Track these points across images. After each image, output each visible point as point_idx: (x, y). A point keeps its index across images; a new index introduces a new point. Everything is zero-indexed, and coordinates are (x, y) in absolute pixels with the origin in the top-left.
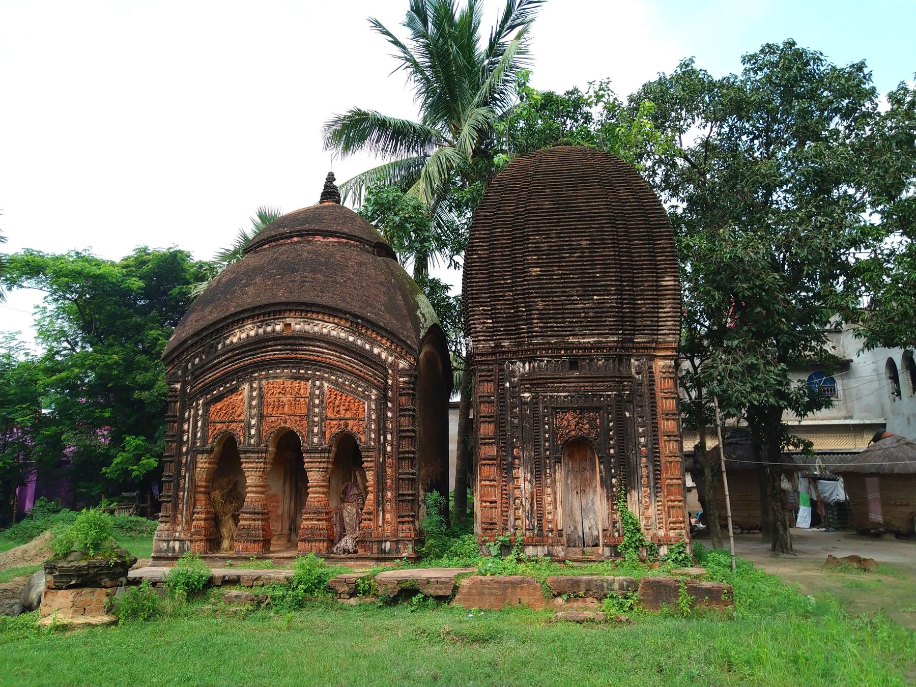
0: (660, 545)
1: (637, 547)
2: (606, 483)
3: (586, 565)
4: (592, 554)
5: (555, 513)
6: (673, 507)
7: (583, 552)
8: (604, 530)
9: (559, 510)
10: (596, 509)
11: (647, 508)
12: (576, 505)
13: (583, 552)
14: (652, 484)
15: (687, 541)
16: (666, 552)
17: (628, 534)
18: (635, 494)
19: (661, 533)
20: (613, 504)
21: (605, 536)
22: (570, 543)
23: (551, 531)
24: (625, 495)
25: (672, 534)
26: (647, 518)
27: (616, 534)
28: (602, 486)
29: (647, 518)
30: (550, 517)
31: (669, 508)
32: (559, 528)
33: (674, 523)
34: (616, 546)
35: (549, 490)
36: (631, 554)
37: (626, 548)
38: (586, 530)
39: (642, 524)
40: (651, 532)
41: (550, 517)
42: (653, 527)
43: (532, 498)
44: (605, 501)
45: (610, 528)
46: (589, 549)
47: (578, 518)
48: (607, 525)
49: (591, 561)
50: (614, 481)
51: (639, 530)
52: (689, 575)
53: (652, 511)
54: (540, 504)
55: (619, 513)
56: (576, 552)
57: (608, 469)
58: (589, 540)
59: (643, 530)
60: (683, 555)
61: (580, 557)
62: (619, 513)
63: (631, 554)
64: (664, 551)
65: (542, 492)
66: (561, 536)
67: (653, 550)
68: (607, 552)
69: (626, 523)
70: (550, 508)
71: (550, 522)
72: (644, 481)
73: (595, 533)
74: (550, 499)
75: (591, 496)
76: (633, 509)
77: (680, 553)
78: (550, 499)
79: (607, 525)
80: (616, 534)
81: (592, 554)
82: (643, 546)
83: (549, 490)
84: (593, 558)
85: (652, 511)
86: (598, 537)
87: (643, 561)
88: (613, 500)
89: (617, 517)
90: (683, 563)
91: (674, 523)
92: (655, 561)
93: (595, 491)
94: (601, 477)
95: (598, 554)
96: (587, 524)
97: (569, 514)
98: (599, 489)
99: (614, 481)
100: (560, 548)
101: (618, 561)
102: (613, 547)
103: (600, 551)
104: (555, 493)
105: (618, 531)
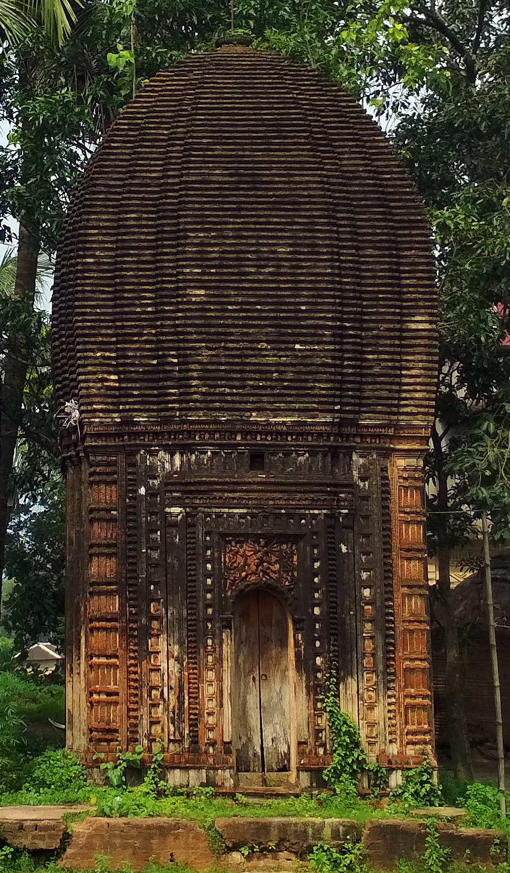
0: (390, 770)
1: (353, 774)
2: (304, 665)
3: (270, 801)
4: (280, 783)
5: (221, 713)
6: (413, 707)
7: (264, 782)
8: (300, 743)
9: (227, 709)
10: (286, 707)
11: (371, 708)
12: (252, 701)
13: (264, 782)
14: (381, 667)
15: (435, 763)
16: (400, 782)
17: (340, 751)
18: (352, 683)
19: (393, 750)
20: (317, 701)
21: (301, 754)
22: (242, 765)
23: (213, 744)
24: (337, 685)
25: (410, 751)
26: (371, 725)
27: (321, 751)
28: (298, 668)
29: (371, 725)
30: (211, 720)
31: (406, 708)
32: (226, 739)
33: (414, 733)
34: (319, 771)
35: (211, 675)
36: (346, 785)
37: (337, 774)
38: (268, 743)
39: (363, 733)
40: (376, 748)
41: (211, 720)
42: (381, 739)
43: (181, 688)
44: (303, 695)
45: (311, 741)
46: (273, 775)
47: (254, 721)
48: (305, 735)
49: (277, 795)
50: (319, 660)
51: (357, 745)
52: (439, 818)
53: (379, 713)
54: (195, 697)
55: (326, 716)
56: (252, 780)
57: (310, 641)
58: (271, 760)
59: (364, 745)
60: (427, 786)
61: (260, 788)
62: (326, 716)
63: (346, 785)
64: (396, 779)
65: (199, 678)
66: (228, 752)
67: (378, 778)
68: (305, 779)
69: (338, 734)
70: (211, 705)
71: (211, 729)
72: (367, 662)
73: (283, 748)
74: (211, 690)
75: (276, 685)
76: (349, 709)
77: (422, 783)
78: (211, 690)
79: (305, 735)
80: (321, 751)
81: (280, 783)
82: (363, 770)
83: (211, 675)
84: (281, 790)
85: (379, 713)
86: (287, 756)
87: (363, 796)
88: (316, 694)
89: (323, 721)
90: (428, 799)
91: (414, 733)
92: (382, 796)
93: (284, 678)
94: (298, 654)
95: (289, 785)
96: (268, 733)
97: (241, 716)
98: (292, 673)
99: (319, 660)
100: (227, 773)
101: (324, 795)
102: (316, 773)
103: (293, 779)
104: (220, 679)
105: (323, 745)
